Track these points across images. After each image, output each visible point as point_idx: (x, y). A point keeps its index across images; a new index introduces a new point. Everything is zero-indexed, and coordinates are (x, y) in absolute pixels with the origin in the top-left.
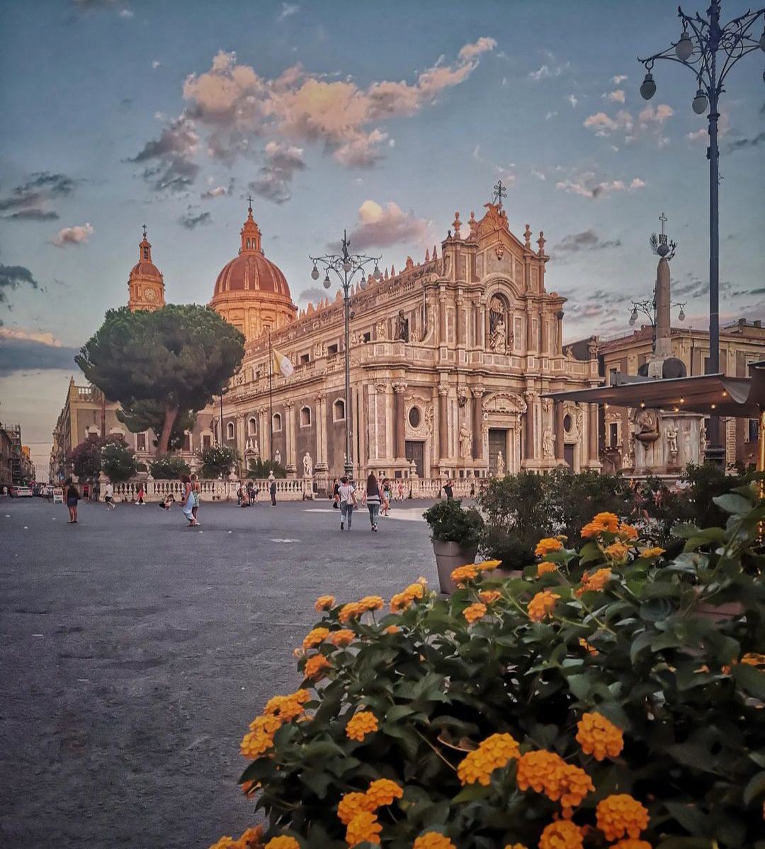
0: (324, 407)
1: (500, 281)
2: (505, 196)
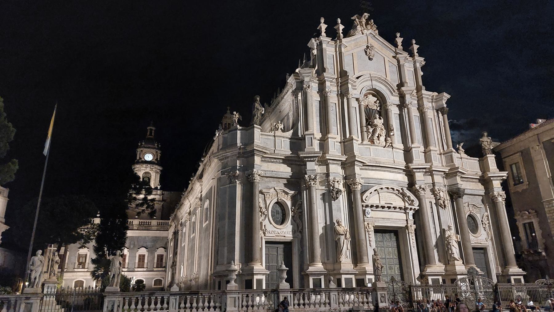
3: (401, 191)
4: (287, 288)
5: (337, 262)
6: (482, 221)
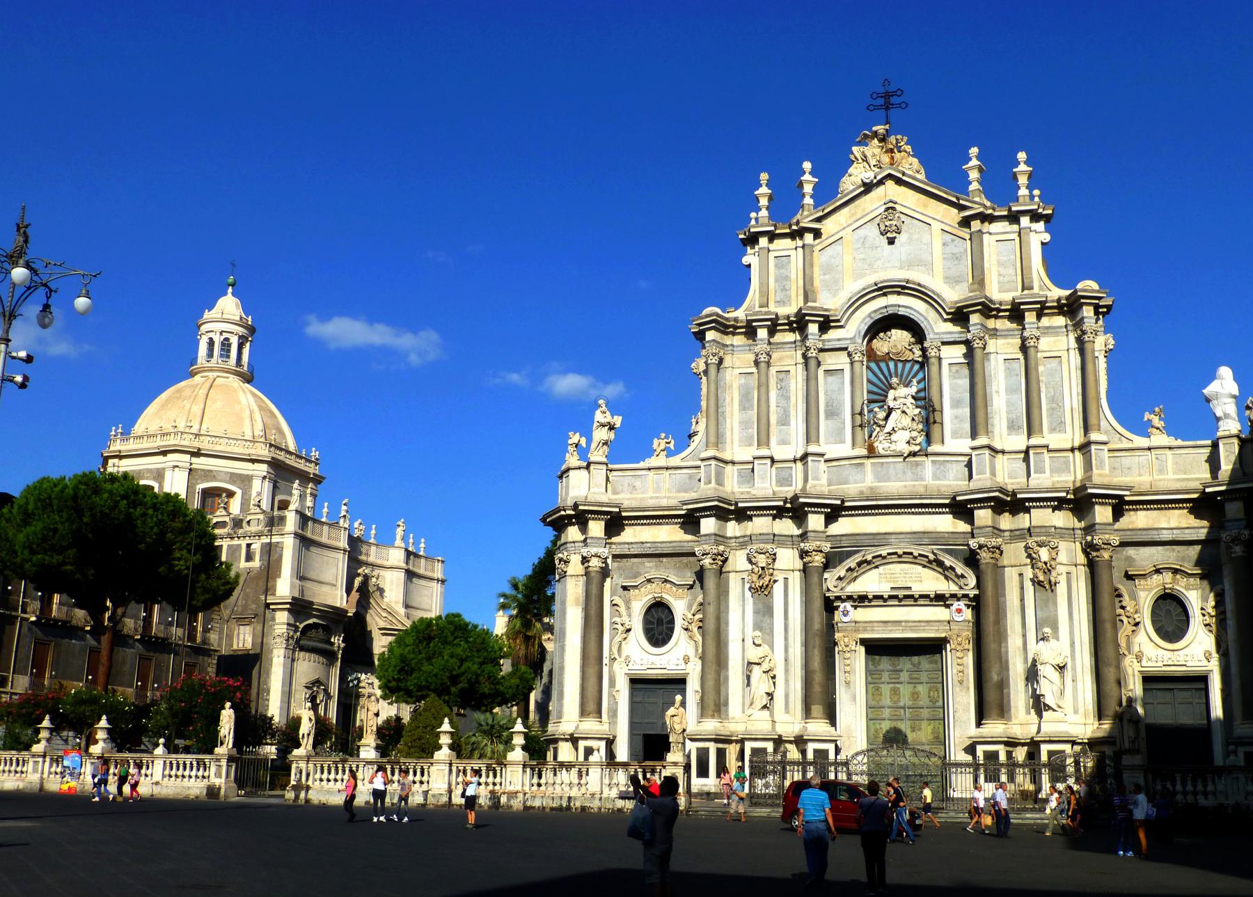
1: (883, 290)
3: (932, 557)
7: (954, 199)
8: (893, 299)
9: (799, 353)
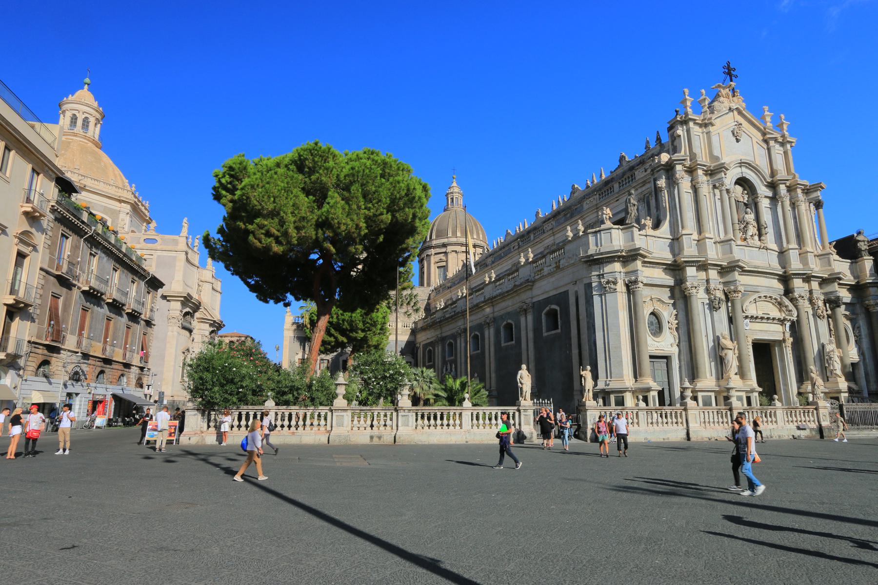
0: (530, 318)
1: (742, 164)
2: (736, 77)
4: (738, 406)
5: (722, 378)
6: (854, 333)
7: (762, 128)
8: (744, 169)
9: (711, 186)
